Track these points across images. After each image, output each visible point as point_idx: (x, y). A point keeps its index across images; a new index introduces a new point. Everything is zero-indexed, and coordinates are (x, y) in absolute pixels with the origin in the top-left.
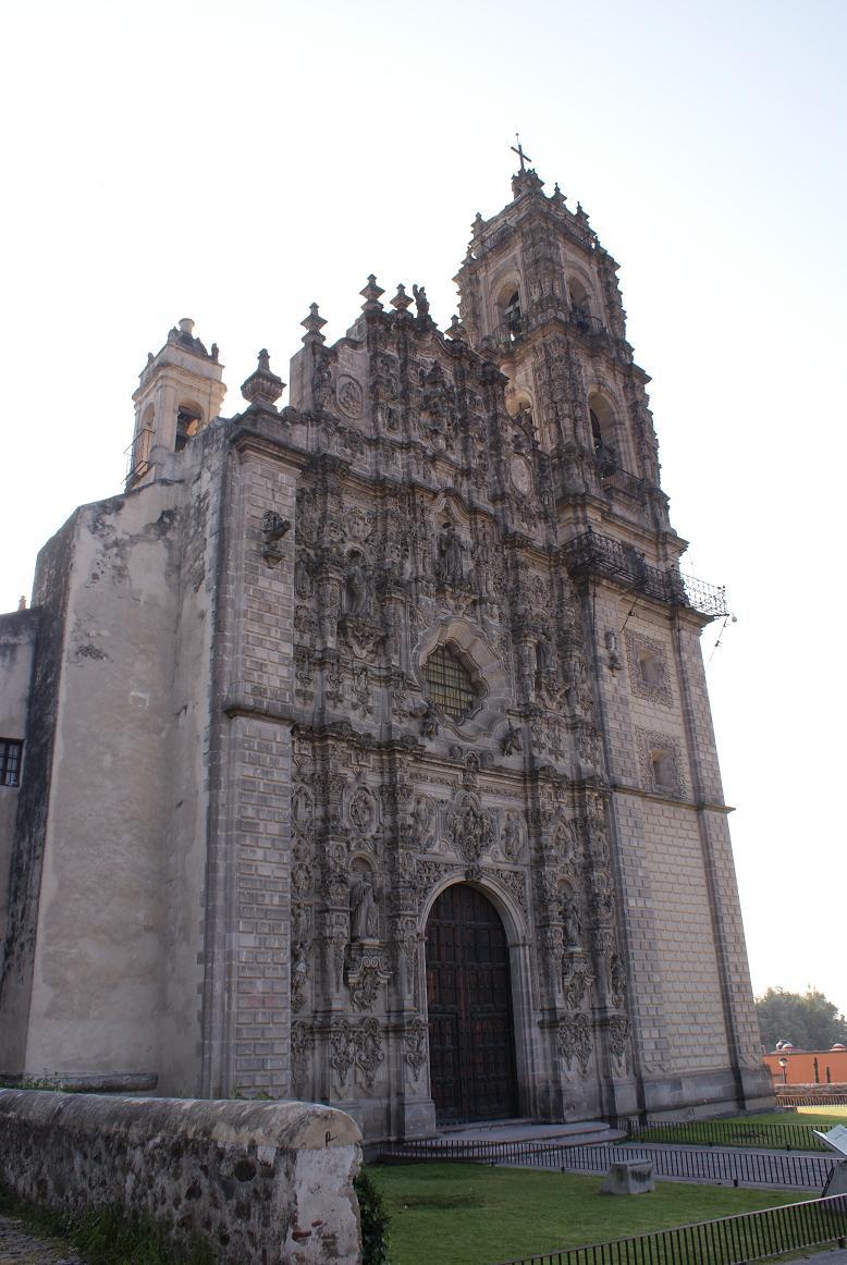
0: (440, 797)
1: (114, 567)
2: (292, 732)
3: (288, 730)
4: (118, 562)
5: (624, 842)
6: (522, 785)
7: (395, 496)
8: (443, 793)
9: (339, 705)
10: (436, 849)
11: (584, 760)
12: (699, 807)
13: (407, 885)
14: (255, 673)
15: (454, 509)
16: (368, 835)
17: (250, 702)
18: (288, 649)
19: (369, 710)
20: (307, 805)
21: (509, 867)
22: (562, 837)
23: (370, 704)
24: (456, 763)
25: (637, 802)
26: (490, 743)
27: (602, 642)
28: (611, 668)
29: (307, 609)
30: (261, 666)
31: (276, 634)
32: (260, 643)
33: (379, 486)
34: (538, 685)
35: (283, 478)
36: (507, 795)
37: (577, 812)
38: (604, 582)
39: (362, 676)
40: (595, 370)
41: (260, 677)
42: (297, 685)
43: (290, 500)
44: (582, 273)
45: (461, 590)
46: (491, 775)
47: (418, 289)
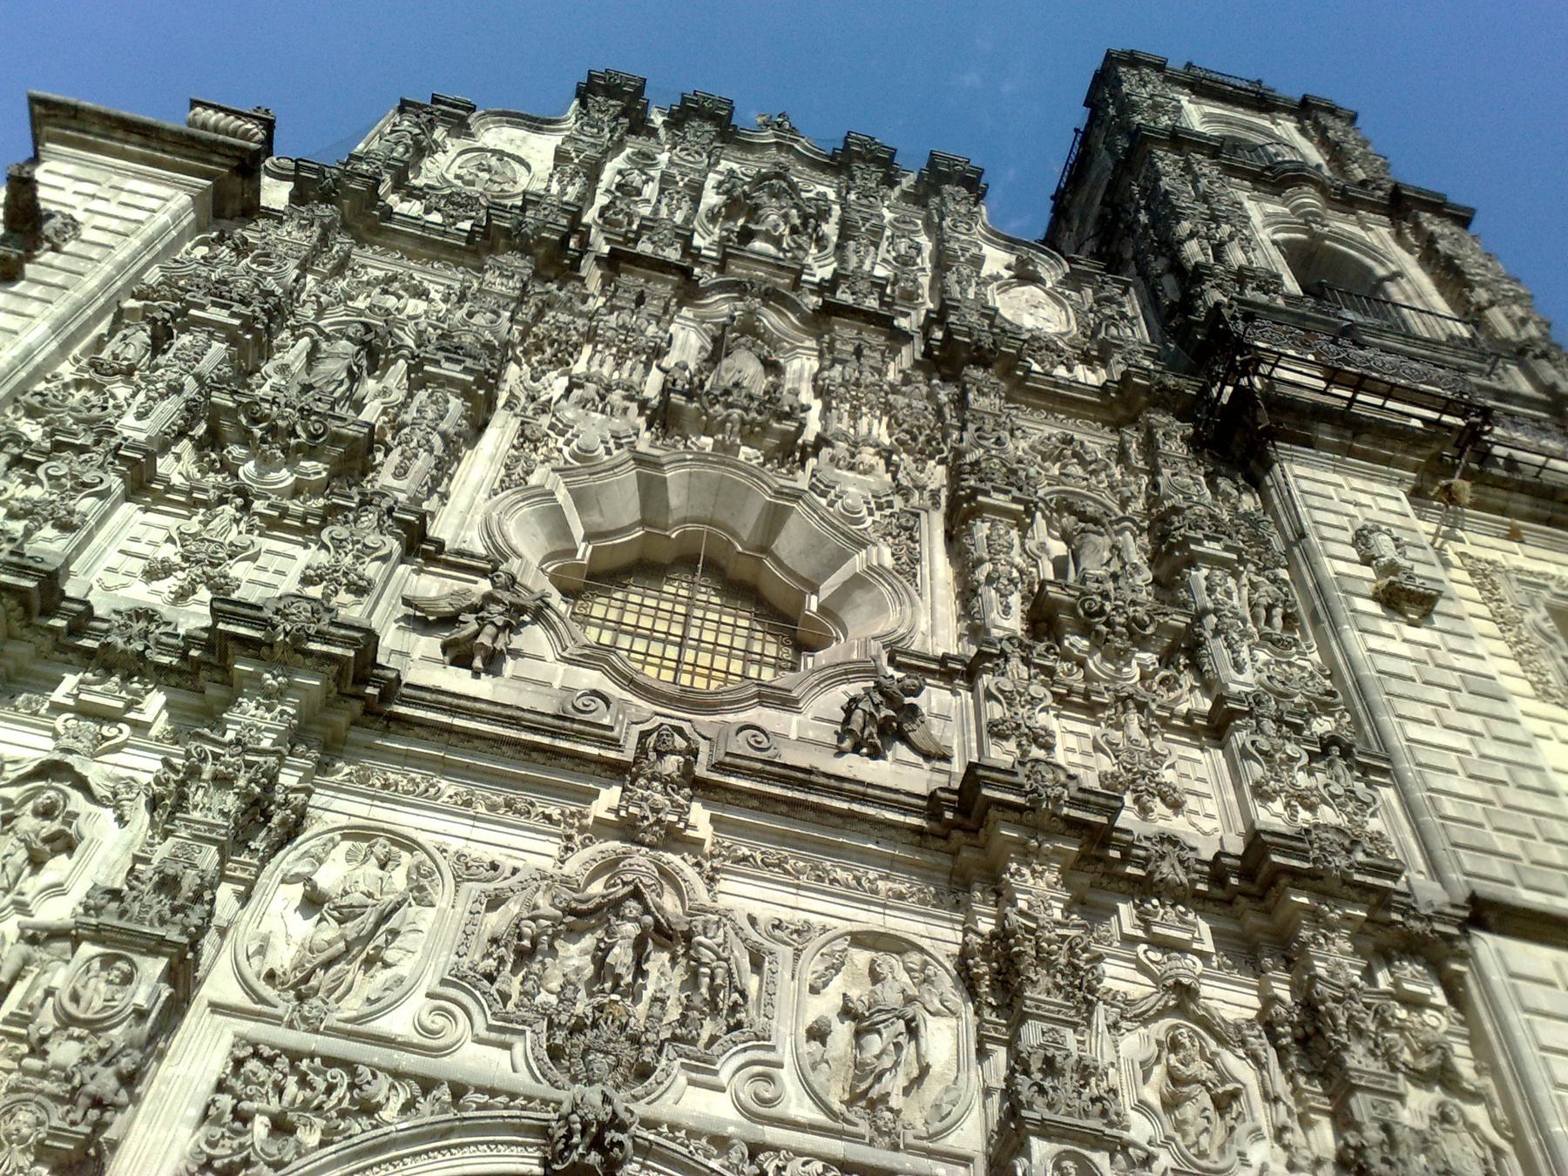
6: (947, 862)
7: (525, 250)
13: (48, 1086)
22: (1199, 1068)
24: (579, 736)
37: (1283, 992)
39: (229, 510)
45: (728, 406)
46: (766, 803)
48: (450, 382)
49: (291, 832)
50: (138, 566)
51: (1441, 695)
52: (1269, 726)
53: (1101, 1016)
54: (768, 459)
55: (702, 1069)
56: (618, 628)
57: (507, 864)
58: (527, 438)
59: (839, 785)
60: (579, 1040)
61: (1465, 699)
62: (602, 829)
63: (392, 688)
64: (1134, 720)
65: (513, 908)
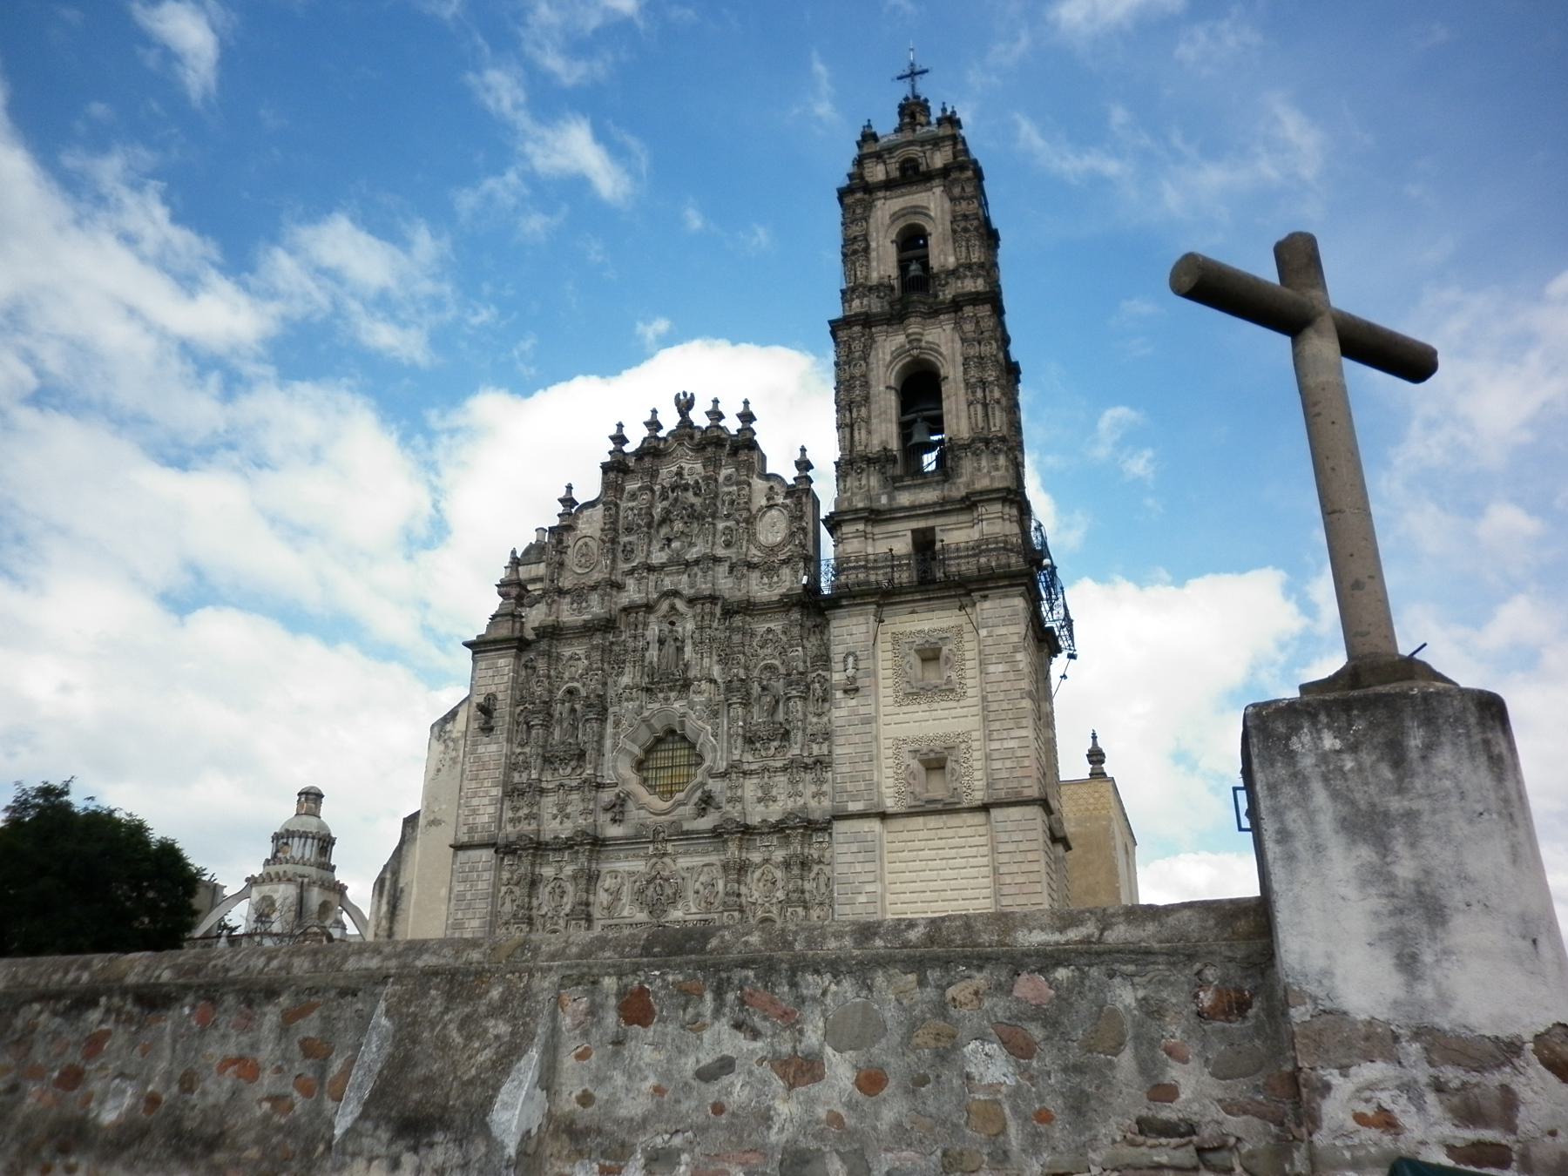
0: (632, 869)
1: (451, 759)
2: (496, 852)
3: (492, 851)
4: (454, 754)
5: (839, 869)
8: (639, 866)
9: (532, 821)
10: (625, 913)
11: (792, 799)
12: (985, 808)
14: (471, 818)
15: (680, 605)
16: (562, 914)
17: (465, 839)
18: (497, 792)
19: (568, 816)
20: (513, 901)
21: (698, 917)
23: (568, 811)
25: (875, 825)
26: (688, 810)
27: (840, 666)
28: (846, 692)
29: (523, 753)
30: (474, 812)
31: (487, 783)
32: (475, 795)
33: (588, 630)
34: (749, 741)
35: (502, 662)
36: (707, 853)
38: (844, 602)
40: (907, 336)
41: (474, 819)
42: (508, 814)
43: (506, 677)
44: (916, 213)
46: (681, 840)
47: (682, 397)
48: (592, 719)
49: (598, 876)
50: (550, 816)
51: (851, 730)
52: (795, 770)
53: (750, 869)
54: (679, 692)
55: (675, 908)
56: (657, 768)
57: (636, 869)
58: (617, 724)
59: (693, 832)
60: (655, 907)
61: (860, 728)
62: (652, 856)
63: (604, 840)
64: (766, 774)
65: (638, 884)
